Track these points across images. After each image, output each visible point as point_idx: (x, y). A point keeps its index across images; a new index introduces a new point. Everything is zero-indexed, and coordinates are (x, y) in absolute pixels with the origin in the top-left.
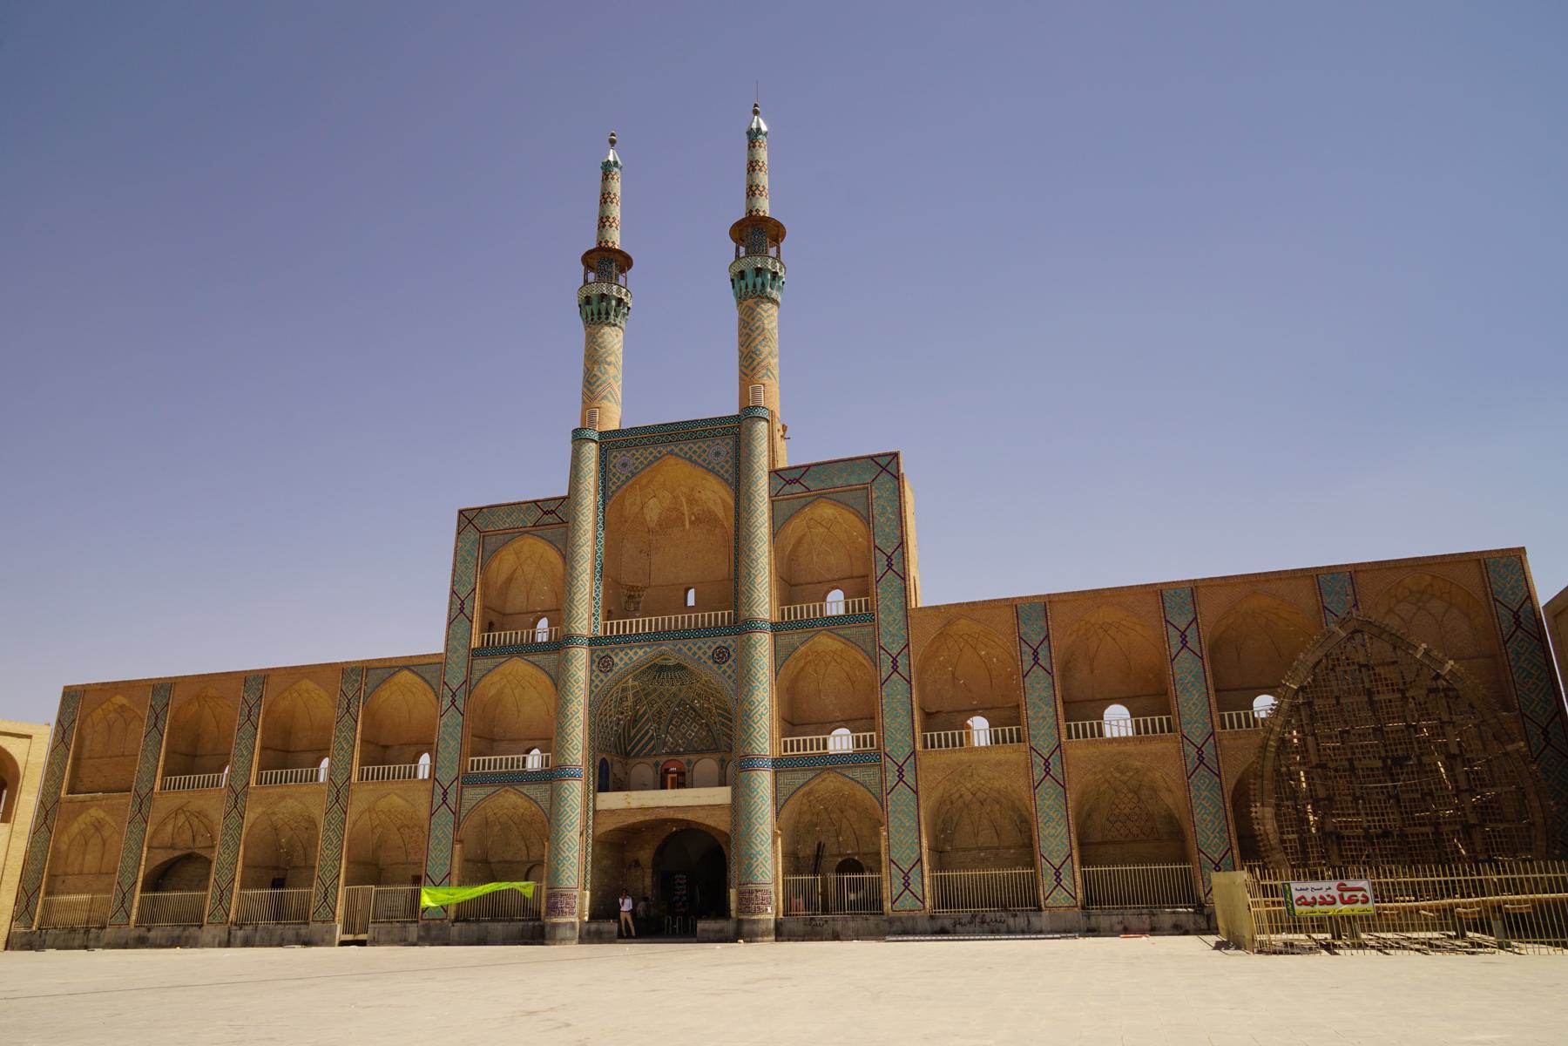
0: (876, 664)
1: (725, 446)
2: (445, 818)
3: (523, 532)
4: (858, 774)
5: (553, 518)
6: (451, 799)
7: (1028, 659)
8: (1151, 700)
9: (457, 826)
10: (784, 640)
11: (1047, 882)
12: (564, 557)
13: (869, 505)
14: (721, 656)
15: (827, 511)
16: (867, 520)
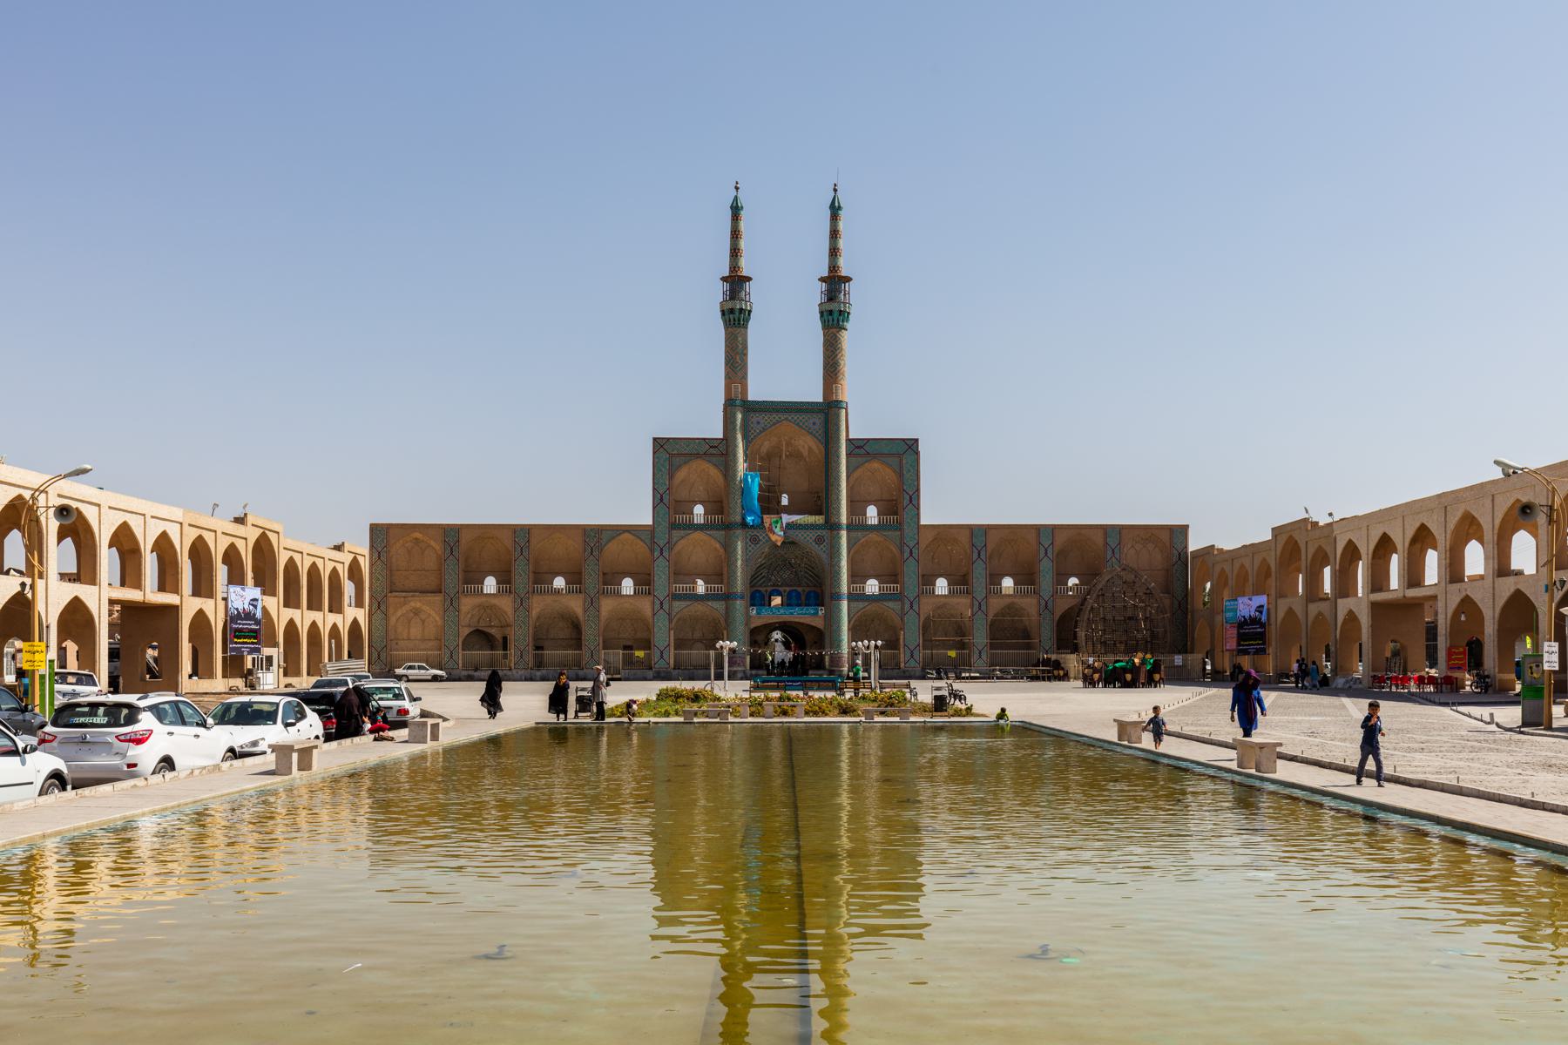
0: (902, 552)
1: (818, 419)
2: (662, 615)
3: (697, 456)
4: (891, 604)
5: (718, 451)
6: (666, 606)
7: (975, 556)
8: (1026, 578)
9: (670, 621)
10: (854, 534)
11: (975, 656)
12: (725, 476)
13: (901, 467)
14: (819, 540)
15: (876, 465)
16: (901, 475)
